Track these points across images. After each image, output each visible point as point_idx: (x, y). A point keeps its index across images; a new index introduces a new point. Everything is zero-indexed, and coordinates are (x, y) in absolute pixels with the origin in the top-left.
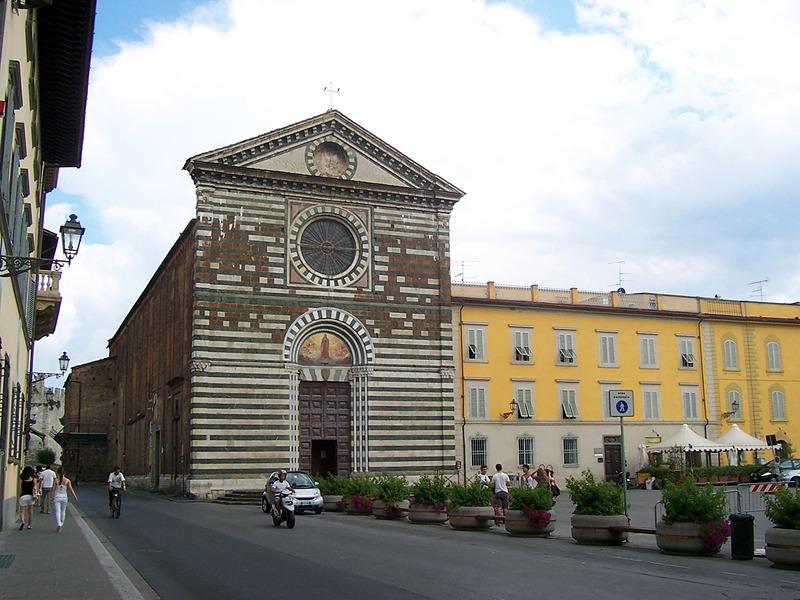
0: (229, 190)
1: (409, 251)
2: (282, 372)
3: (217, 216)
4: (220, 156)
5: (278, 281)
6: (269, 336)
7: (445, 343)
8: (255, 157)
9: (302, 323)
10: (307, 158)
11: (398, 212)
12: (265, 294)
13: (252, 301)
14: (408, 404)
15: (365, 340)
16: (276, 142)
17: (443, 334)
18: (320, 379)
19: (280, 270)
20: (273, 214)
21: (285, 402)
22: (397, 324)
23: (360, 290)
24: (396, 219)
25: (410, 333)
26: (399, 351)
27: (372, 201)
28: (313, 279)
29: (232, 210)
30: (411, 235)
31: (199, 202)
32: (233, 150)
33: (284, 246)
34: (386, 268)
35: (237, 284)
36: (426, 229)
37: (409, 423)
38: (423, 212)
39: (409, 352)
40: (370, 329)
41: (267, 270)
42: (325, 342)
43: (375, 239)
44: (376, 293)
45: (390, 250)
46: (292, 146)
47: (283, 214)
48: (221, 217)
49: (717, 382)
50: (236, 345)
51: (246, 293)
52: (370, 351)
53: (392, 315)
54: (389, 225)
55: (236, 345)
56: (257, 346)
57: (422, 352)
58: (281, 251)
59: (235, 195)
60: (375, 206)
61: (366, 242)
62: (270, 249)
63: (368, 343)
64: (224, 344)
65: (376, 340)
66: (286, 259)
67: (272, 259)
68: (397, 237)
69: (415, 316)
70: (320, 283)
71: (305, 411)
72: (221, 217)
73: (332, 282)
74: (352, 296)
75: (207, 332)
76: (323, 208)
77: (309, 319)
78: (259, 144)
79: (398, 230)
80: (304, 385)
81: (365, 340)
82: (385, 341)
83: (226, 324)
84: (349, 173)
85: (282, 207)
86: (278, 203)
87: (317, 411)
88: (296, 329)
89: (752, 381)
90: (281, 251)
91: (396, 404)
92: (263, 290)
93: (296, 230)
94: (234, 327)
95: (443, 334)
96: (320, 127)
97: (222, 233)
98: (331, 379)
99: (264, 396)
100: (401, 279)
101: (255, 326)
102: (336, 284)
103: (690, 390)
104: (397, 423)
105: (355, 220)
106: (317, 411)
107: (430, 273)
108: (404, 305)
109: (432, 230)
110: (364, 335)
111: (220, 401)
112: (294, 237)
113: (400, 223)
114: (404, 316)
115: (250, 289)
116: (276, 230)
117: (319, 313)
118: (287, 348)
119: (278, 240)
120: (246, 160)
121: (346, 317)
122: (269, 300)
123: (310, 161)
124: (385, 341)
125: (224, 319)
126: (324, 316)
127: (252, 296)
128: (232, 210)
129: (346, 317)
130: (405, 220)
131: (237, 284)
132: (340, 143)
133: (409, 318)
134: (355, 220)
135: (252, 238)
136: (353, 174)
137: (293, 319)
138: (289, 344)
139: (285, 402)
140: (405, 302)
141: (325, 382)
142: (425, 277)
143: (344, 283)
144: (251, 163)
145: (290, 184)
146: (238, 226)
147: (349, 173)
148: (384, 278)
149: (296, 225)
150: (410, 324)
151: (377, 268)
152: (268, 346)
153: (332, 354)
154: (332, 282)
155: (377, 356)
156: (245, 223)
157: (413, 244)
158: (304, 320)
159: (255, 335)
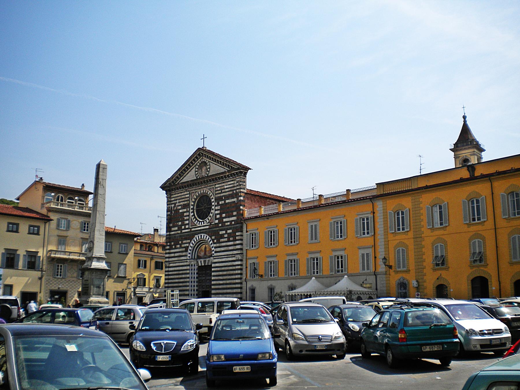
0: (175, 194)
1: (227, 201)
2: (187, 263)
3: (171, 206)
4: (168, 183)
5: (187, 227)
6: (184, 249)
7: (237, 242)
8: (180, 178)
9: (193, 242)
10: (196, 171)
11: (223, 184)
12: (184, 233)
13: (180, 236)
14: (225, 273)
15: (212, 246)
16: (184, 170)
17: (237, 238)
18: (203, 265)
19: (187, 222)
20: (186, 199)
21: (188, 276)
22: (222, 236)
23: (211, 223)
24: (223, 188)
25: (226, 239)
26: (222, 249)
27: (214, 183)
28: (197, 223)
29: (175, 202)
30: (227, 193)
31: (167, 202)
32: (172, 179)
33: (189, 211)
34: (218, 212)
35: (177, 230)
36: (233, 189)
37: (225, 282)
38: (232, 181)
39: (226, 248)
40: (213, 240)
41: (184, 223)
42: (205, 248)
43: (215, 200)
44: (215, 224)
45: (220, 203)
46: (191, 169)
47: (188, 199)
48: (173, 205)
49: (387, 243)
50: (176, 255)
51: (178, 233)
52: (213, 250)
53: (221, 233)
54: (220, 192)
55: (176, 255)
56: (181, 254)
57: (231, 248)
58: (188, 214)
59: (176, 195)
60: (216, 185)
61: (213, 202)
62: (185, 214)
63: (213, 247)
64: (173, 255)
65: (215, 245)
66: (189, 218)
67: (185, 218)
68: (223, 196)
69: (229, 231)
70: (199, 224)
71: (200, 278)
72: (173, 205)
73: (203, 223)
74: (208, 227)
75: (168, 251)
76: (200, 191)
77: (195, 241)
78: (179, 173)
79: (224, 192)
80: (200, 268)
81: (212, 246)
82: (218, 245)
83: (174, 247)
84: (208, 173)
85: (188, 196)
86: (187, 194)
87: (204, 278)
88: (192, 245)
89: (418, 238)
90: (188, 214)
91: (221, 273)
92: (183, 231)
93: (193, 203)
94: (176, 248)
95: (237, 238)
96: (196, 157)
97: (173, 212)
98: (206, 264)
99: (182, 274)
100: (224, 215)
101: (181, 247)
102: (204, 223)
103: (365, 252)
104: (221, 282)
105: (210, 193)
106: (204, 278)
107: (234, 209)
108: (224, 227)
109: (235, 188)
110: (212, 244)
111: (172, 277)
112: (192, 207)
113: (224, 189)
114: (224, 232)
115: (179, 232)
116: (187, 206)
117: (198, 237)
118: (190, 253)
119: (187, 210)
120: (178, 180)
121: (206, 237)
122: (184, 235)
123: (197, 173)
124: (218, 245)
125: (173, 245)
126: (200, 238)
127: (180, 235)
128: (175, 202)
129: (206, 237)
130: (226, 187)
131: (177, 230)
132: (205, 161)
133: (226, 233)
134: (210, 193)
135: (180, 211)
136: (209, 173)
137: (191, 241)
138: (190, 252)
139: (188, 276)
140: (225, 226)
141: (205, 266)
142: (232, 212)
143: (206, 222)
144: (180, 181)
145: (188, 186)
146: (177, 207)
147: (208, 173)
148: (218, 216)
149: (193, 202)
150: (226, 236)
151: (216, 212)
152: (184, 254)
153: (207, 253)
154: (203, 223)
155: (216, 252)
156: (179, 206)
157: (228, 197)
158: (194, 241)
159: (181, 250)
